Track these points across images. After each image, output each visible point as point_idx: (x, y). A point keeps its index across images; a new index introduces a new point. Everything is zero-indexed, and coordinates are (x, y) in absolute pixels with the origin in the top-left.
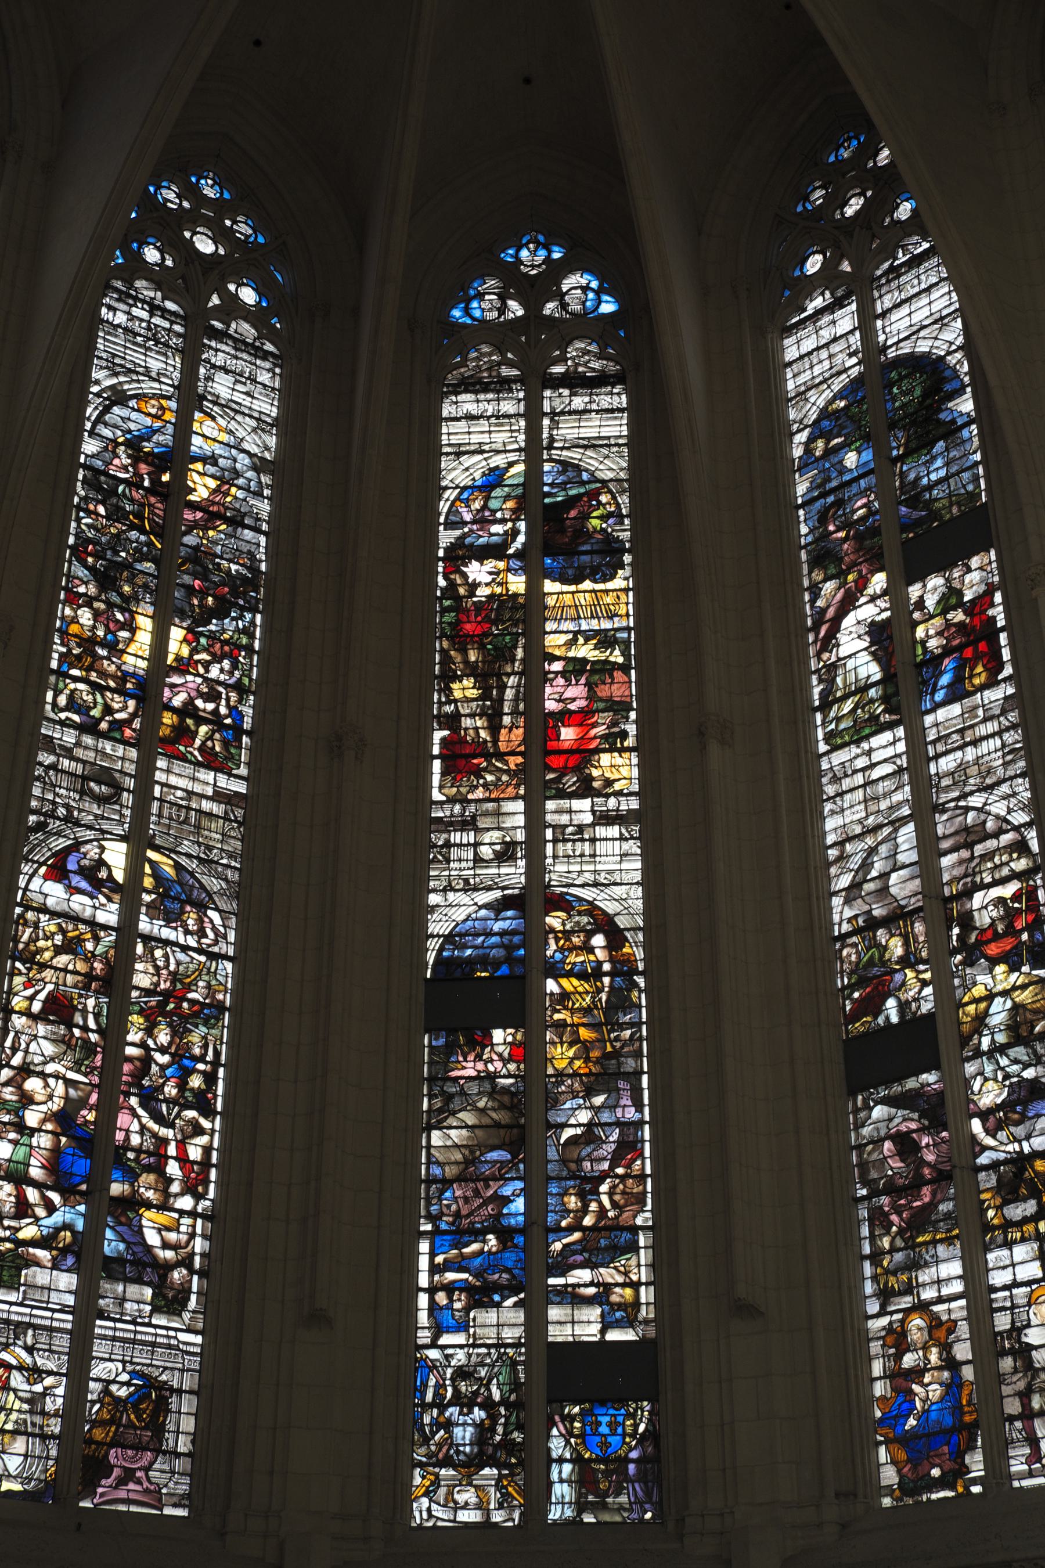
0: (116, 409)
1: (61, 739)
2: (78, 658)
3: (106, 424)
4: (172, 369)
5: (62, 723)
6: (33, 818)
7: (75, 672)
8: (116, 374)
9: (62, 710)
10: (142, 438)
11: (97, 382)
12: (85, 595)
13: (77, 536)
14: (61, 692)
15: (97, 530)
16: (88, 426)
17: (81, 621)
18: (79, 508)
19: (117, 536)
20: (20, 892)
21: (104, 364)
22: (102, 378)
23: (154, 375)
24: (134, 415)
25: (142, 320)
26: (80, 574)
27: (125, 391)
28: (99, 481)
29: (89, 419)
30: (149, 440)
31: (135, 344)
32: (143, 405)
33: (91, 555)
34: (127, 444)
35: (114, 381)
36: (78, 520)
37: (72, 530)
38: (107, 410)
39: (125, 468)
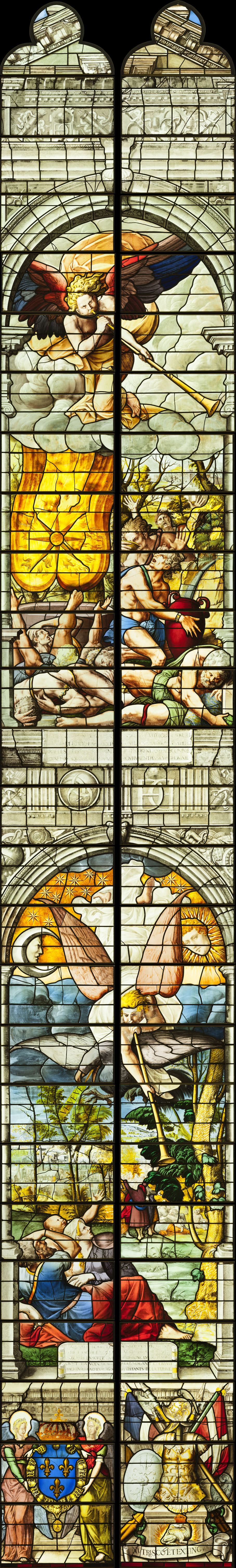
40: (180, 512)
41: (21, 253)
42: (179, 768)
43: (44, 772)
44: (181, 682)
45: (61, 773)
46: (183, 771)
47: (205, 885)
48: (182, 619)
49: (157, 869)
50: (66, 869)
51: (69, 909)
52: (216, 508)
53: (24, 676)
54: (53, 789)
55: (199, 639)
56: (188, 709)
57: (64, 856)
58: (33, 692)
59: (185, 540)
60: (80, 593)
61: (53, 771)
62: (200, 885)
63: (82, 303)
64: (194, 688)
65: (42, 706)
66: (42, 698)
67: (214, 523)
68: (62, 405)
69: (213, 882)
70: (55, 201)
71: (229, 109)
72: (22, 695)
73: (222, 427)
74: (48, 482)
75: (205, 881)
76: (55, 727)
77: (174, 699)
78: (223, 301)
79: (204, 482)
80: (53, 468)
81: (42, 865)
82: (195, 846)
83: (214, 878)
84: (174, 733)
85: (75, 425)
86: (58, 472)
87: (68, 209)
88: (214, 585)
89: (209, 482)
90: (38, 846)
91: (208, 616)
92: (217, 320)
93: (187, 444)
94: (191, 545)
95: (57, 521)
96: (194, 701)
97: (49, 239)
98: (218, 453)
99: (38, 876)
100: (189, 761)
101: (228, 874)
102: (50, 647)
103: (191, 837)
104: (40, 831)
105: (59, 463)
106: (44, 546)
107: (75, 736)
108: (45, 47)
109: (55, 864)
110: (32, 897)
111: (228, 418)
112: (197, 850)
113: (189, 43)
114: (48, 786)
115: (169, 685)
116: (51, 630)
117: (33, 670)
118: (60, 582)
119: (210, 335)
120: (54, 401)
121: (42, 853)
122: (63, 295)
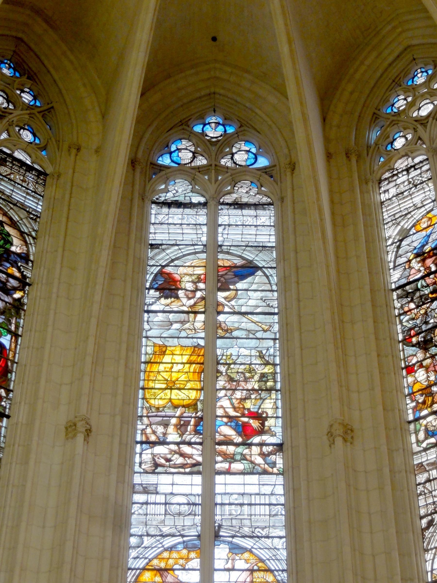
0: (404, 243)
1: (427, 460)
2: (424, 403)
3: (400, 256)
4: (429, 193)
5: (425, 450)
6: (424, 522)
7: (425, 412)
8: (398, 224)
9: (423, 441)
10: (423, 246)
11: (390, 238)
12: (418, 362)
13: (403, 332)
14: (419, 430)
15: (413, 319)
16: (391, 265)
17: (419, 380)
18: (400, 315)
19: (426, 313)
20: (429, 574)
21: (391, 224)
22: (391, 232)
23: (419, 205)
24: (414, 237)
25: (404, 182)
26: (411, 352)
27: (406, 229)
28: (407, 291)
29: (390, 262)
30: (427, 243)
31: (404, 198)
32: (419, 228)
33: (414, 336)
34: (417, 255)
35: (399, 227)
36: (401, 322)
37: (399, 331)
38: (399, 247)
39: (419, 271)
40: (250, 372)
41: (157, 266)
42: (251, 495)
43: (158, 496)
44: (251, 452)
45: (168, 497)
46: (253, 497)
47: (269, 560)
48: (251, 421)
49: (236, 549)
50: (171, 549)
51: (171, 572)
52: (270, 371)
53: (148, 447)
54: (164, 506)
55: (261, 432)
56: (256, 464)
57: (169, 542)
58: (154, 455)
59: (254, 384)
60: (184, 409)
61: (164, 496)
62: (265, 559)
63: (190, 286)
64: (259, 455)
65: (158, 463)
66: (158, 458)
67: (269, 378)
68: (176, 326)
69: (273, 558)
70: (176, 248)
71: (272, 218)
72: (147, 457)
73: (273, 337)
74: (167, 358)
75: (268, 557)
76: (166, 473)
77: (246, 460)
78: (271, 286)
79: (263, 360)
80: (170, 353)
81: (155, 547)
82: (262, 537)
83: (274, 555)
84: (247, 477)
85: (183, 334)
86: (173, 354)
87: (182, 250)
88: (271, 406)
89: (266, 360)
90: (152, 536)
91: (267, 420)
92: (269, 294)
93: (253, 343)
94: (256, 387)
95: (171, 375)
96: (259, 460)
97: (173, 261)
98: (271, 347)
99: (151, 554)
100: (257, 491)
101: (283, 554)
102: (165, 434)
103: (259, 532)
104: (154, 528)
105: (174, 351)
106: (164, 386)
107: (178, 479)
108: (174, 194)
109: (163, 546)
110: (147, 564)
111: (275, 333)
112: (263, 539)
113: (252, 193)
114: (160, 504)
115: (244, 453)
116: (166, 425)
117: (154, 444)
118: (172, 403)
119: (265, 300)
120: (172, 325)
121: (155, 540)
122: (178, 283)
